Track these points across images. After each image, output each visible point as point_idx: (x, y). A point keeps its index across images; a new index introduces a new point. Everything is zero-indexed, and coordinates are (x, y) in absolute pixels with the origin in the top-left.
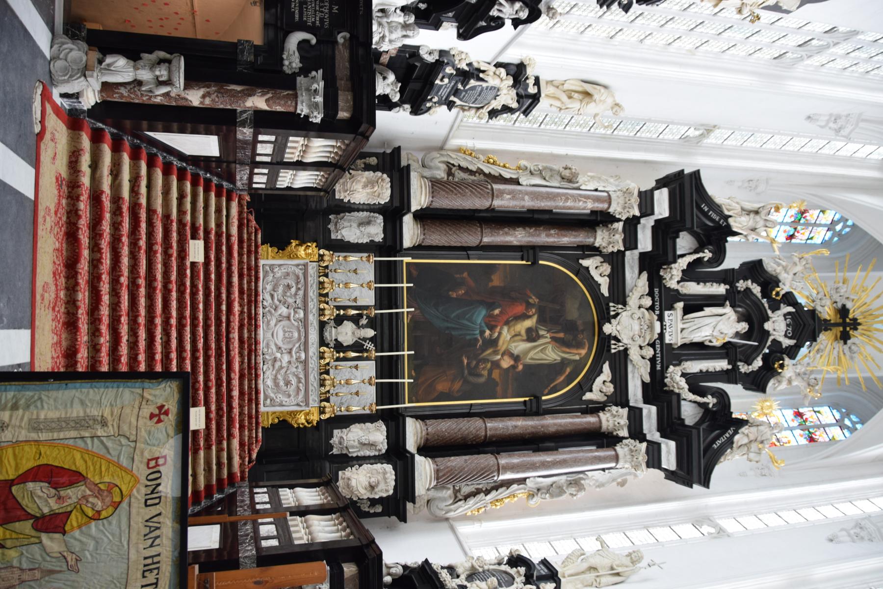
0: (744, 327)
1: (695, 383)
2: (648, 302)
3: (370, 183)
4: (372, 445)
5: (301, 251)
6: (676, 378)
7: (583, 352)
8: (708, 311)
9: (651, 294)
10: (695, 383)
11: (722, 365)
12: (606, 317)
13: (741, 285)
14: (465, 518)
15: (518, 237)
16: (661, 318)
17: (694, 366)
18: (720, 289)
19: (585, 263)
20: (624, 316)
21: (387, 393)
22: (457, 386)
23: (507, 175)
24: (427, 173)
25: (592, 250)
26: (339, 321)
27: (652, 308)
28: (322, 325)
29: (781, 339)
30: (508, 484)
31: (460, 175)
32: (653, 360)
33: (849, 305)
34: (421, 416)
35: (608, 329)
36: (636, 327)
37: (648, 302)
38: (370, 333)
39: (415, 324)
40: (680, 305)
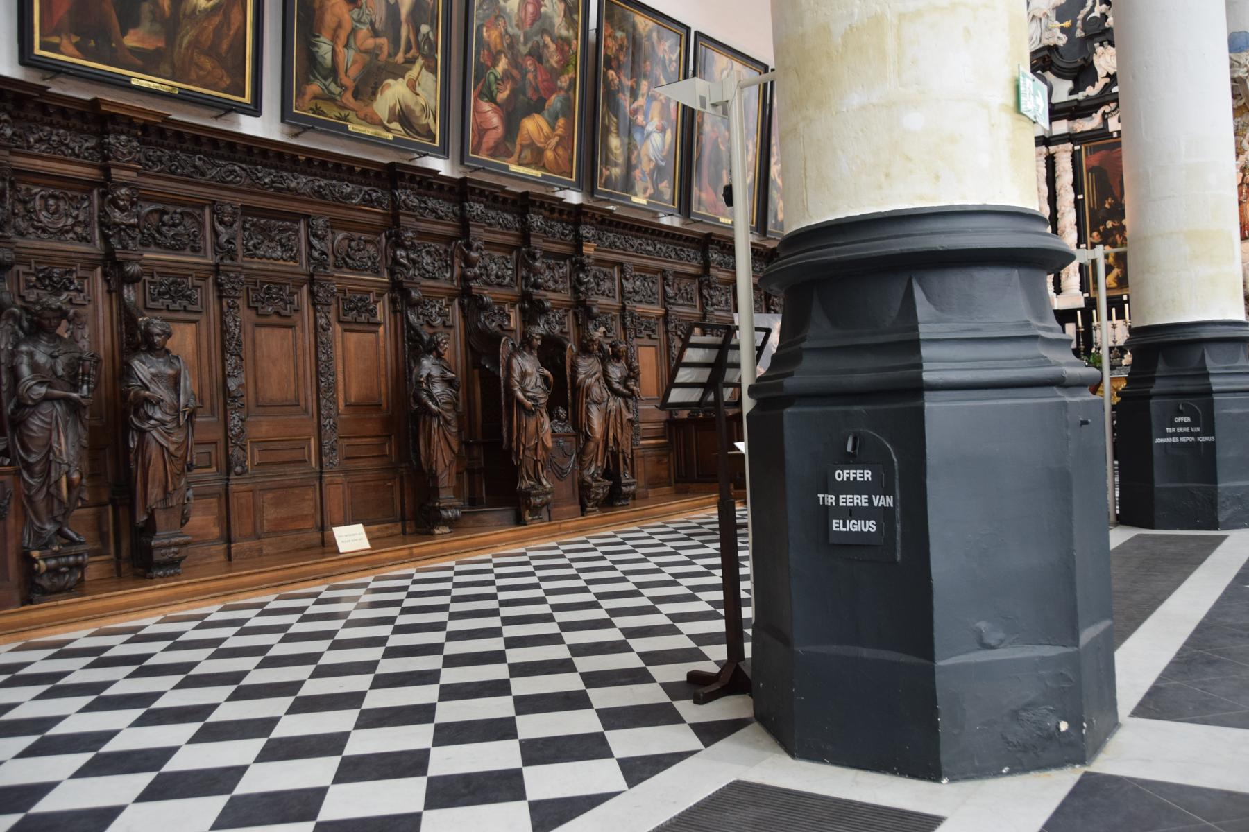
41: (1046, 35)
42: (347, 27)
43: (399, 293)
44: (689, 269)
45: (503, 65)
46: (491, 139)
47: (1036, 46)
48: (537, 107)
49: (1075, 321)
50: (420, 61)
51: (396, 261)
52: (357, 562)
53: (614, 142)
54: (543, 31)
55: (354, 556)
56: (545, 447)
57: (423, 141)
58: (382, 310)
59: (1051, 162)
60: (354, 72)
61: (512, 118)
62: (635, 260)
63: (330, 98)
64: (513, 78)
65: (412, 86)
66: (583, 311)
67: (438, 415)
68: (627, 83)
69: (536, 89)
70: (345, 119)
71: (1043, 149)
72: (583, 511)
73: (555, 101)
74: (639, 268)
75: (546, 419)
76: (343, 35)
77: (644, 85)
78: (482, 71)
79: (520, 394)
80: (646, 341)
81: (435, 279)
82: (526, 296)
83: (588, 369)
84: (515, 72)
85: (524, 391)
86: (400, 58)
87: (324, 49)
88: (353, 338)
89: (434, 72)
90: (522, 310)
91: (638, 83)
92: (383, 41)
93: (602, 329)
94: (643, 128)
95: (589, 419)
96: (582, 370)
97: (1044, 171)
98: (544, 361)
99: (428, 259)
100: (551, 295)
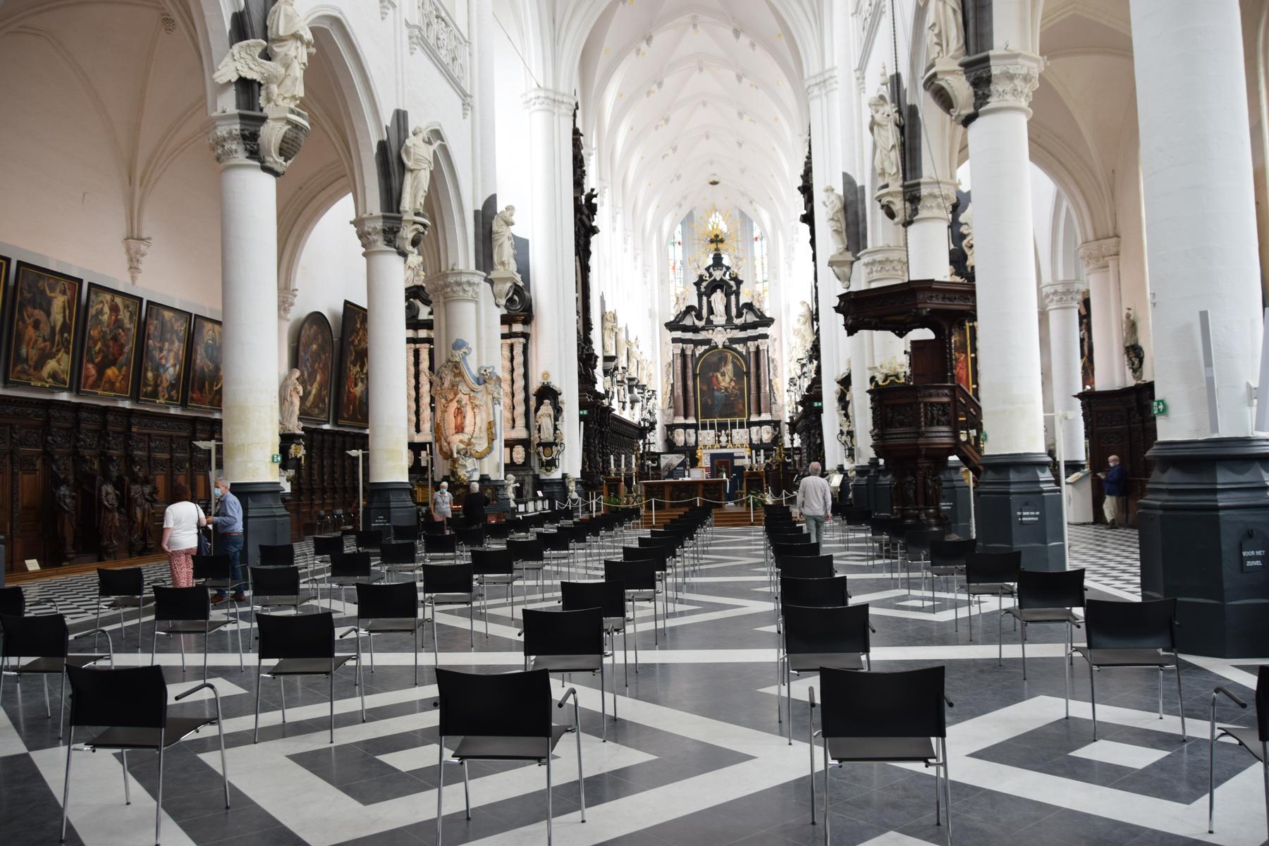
0: (719, 290)
1: (739, 315)
2: (711, 331)
3: (678, 435)
4: (757, 431)
5: (699, 454)
6: (737, 321)
7: (729, 354)
8: (713, 305)
9: (708, 330)
10: (739, 315)
11: (733, 297)
12: (716, 347)
13: (703, 290)
14: (783, 400)
15: (690, 383)
16: (716, 326)
17: (734, 311)
18: (705, 299)
19: (697, 355)
20: (716, 340)
21: (741, 426)
22: (740, 401)
23: (670, 388)
24: (672, 415)
25: (693, 354)
26: (719, 442)
27: (713, 330)
28: (721, 447)
29: (723, 272)
30: (771, 386)
31: (671, 404)
32: (731, 329)
33: (709, 239)
34: (749, 414)
35: (720, 346)
36: (720, 336)
37: (711, 331)
38: (723, 432)
39: (721, 417)
40: (711, 317)
41: (416, 278)
42: (34, 340)
43: (48, 456)
44: (184, 434)
45: (99, 345)
46: (91, 380)
47: (410, 284)
48: (113, 363)
49: (426, 450)
50: (63, 350)
51: (47, 442)
52: (35, 575)
53: (150, 375)
54: (119, 327)
55: (34, 572)
56: (115, 526)
57: (62, 386)
58: (39, 464)
59: (417, 353)
60: (34, 359)
61: (101, 370)
62: (157, 432)
63: (24, 372)
64: (103, 351)
65: (58, 362)
66: (129, 460)
67: (68, 512)
68: (158, 345)
69: (113, 355)
70: (30, 380)
71: (412, 346)
72: (130, 556)
73: (123, 359)
74: (158, 435)
75: (117, 514)
76: (31, 343)
77: (167, 345)
78: (89, 349)
79: (106, 503)
80: (160, 472)
81: (62, 448)
82: (103, 454)
83: (136, 489)
84: (104, 348)
85: (107, 501)
86: (54, 350)
87: (24, 351)
88: (26, 477)
89: (68, 353)
90: (101, 461)
91: (163, 345)
92: (48, 343)
93: (138, 467)
94: (164, 366)
95: (135, 513)
96: (133, 491)
97: (412, 359)
98: (116, 487)
99: (59, 439)
100: (115, 452)
